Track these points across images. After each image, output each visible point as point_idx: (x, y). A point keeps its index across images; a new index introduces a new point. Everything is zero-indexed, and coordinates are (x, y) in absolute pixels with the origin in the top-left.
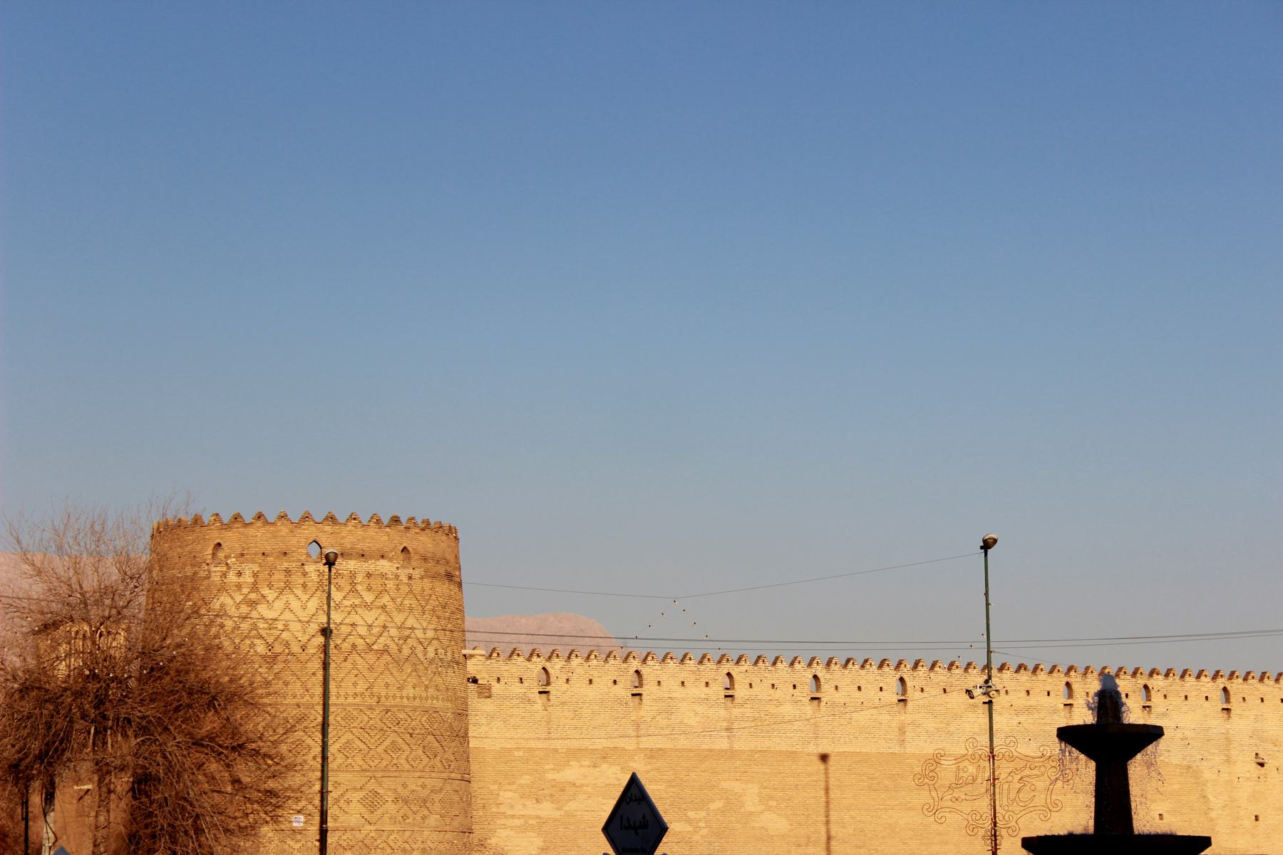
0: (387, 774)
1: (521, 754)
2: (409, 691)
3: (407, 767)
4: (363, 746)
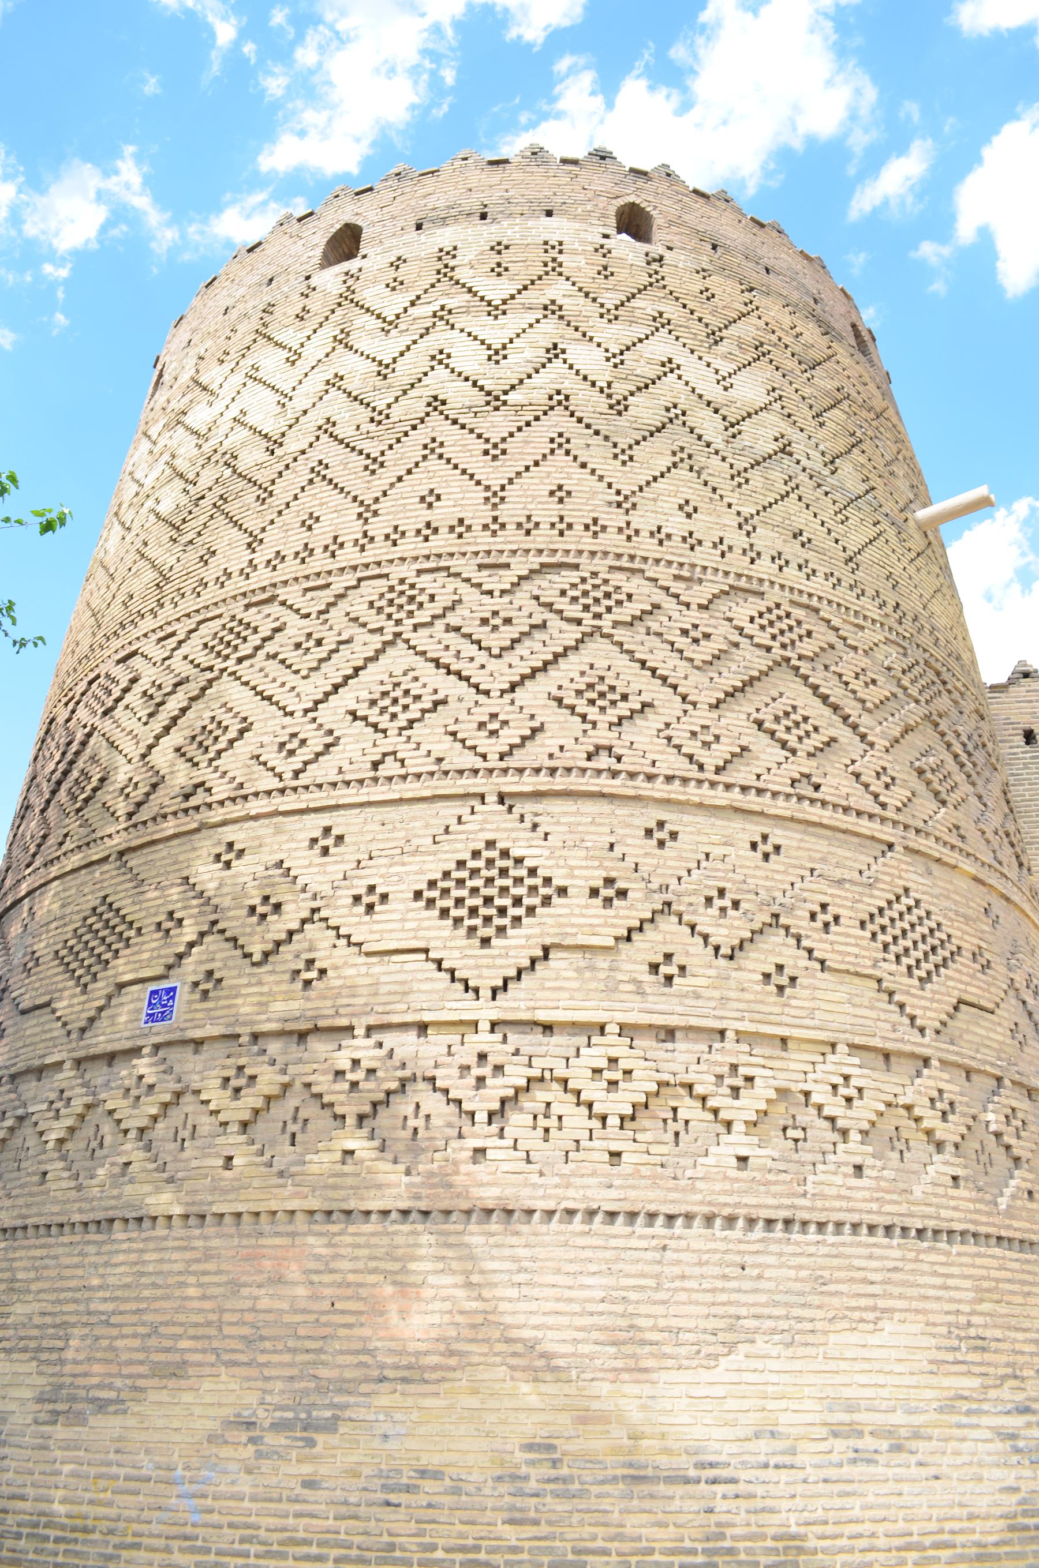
0: (560, 782)
3: (671, 762)
4: (450, 687)
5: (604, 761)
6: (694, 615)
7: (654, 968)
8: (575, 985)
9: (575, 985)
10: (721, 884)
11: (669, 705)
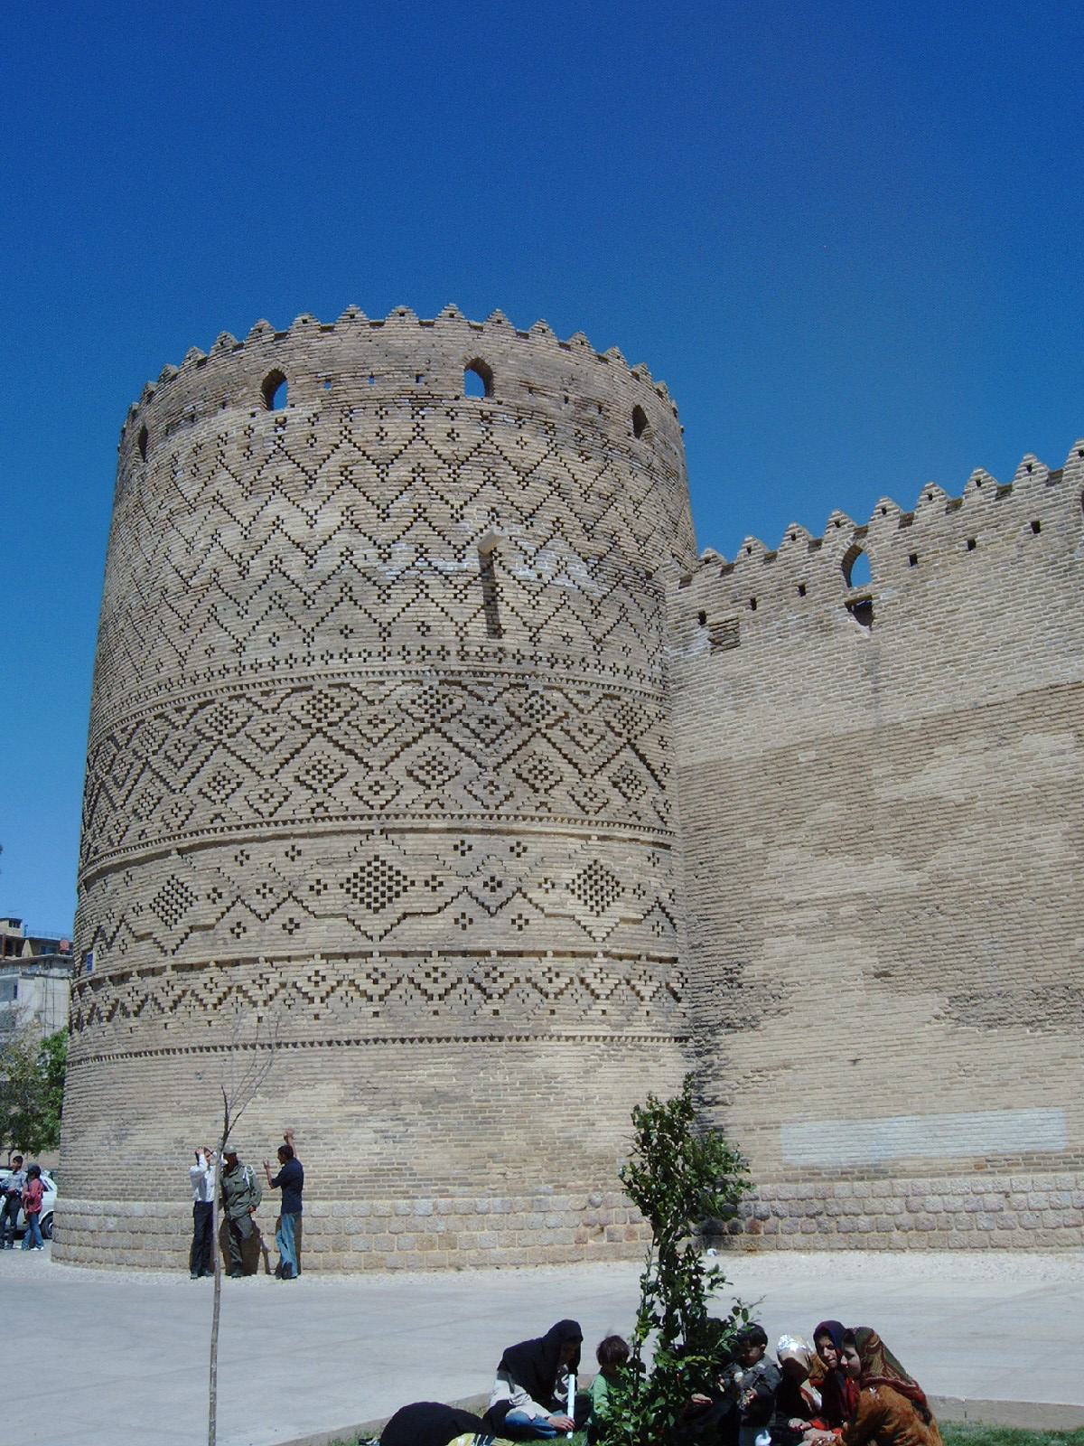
1: (812, 754)
2: (259, 651)
5: (218, 823)
6: (270, 717)
7: (232, 931)
8: (202, 944)
9: (202, 944)
10: (264, 881)
11: (250, 779)
